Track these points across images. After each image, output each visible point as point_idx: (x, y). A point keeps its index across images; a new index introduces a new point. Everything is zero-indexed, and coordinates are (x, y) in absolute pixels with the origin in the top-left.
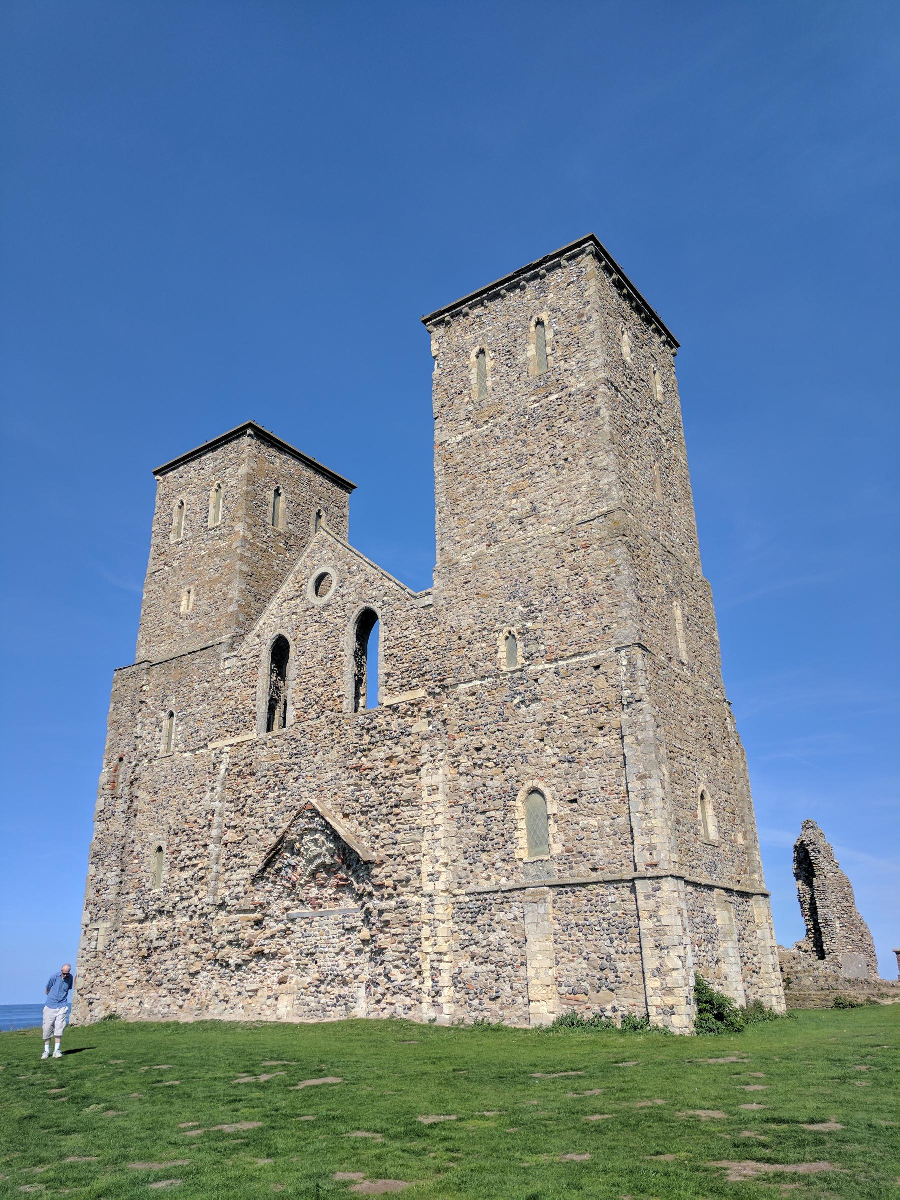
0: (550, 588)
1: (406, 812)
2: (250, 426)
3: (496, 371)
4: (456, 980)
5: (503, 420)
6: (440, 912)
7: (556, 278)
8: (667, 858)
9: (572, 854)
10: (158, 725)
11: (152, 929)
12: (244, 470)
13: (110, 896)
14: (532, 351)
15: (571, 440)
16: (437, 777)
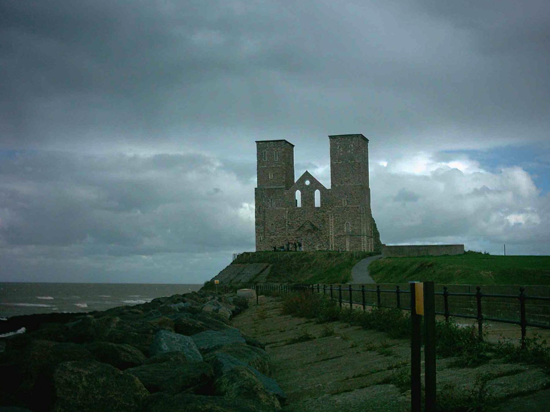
0: (351, 194)
1: (327, 223)
2: (284, 140)
3: (342, 152)
4: (335, 246)
5: (344, 162)
6: (333, 238)
7: (354, 138)
8: (366, 234)
9: (352, 232)
10: (268, 201)
11: (272, 237)
12: (283, 150)
13: (263, 231)
14: (349, 151)
15: (356, 170)
16: (331, 219)
